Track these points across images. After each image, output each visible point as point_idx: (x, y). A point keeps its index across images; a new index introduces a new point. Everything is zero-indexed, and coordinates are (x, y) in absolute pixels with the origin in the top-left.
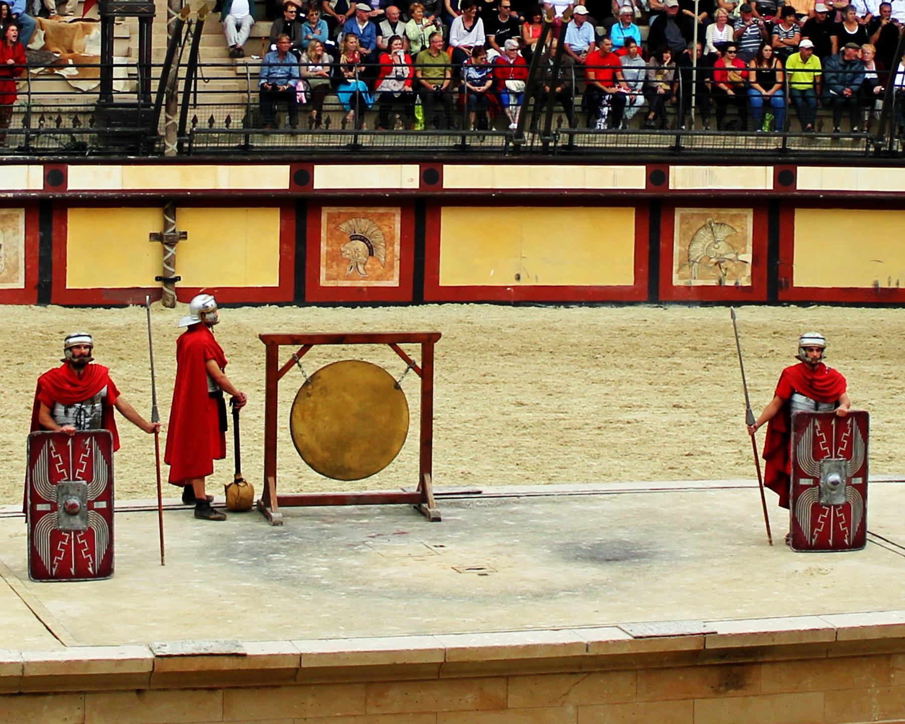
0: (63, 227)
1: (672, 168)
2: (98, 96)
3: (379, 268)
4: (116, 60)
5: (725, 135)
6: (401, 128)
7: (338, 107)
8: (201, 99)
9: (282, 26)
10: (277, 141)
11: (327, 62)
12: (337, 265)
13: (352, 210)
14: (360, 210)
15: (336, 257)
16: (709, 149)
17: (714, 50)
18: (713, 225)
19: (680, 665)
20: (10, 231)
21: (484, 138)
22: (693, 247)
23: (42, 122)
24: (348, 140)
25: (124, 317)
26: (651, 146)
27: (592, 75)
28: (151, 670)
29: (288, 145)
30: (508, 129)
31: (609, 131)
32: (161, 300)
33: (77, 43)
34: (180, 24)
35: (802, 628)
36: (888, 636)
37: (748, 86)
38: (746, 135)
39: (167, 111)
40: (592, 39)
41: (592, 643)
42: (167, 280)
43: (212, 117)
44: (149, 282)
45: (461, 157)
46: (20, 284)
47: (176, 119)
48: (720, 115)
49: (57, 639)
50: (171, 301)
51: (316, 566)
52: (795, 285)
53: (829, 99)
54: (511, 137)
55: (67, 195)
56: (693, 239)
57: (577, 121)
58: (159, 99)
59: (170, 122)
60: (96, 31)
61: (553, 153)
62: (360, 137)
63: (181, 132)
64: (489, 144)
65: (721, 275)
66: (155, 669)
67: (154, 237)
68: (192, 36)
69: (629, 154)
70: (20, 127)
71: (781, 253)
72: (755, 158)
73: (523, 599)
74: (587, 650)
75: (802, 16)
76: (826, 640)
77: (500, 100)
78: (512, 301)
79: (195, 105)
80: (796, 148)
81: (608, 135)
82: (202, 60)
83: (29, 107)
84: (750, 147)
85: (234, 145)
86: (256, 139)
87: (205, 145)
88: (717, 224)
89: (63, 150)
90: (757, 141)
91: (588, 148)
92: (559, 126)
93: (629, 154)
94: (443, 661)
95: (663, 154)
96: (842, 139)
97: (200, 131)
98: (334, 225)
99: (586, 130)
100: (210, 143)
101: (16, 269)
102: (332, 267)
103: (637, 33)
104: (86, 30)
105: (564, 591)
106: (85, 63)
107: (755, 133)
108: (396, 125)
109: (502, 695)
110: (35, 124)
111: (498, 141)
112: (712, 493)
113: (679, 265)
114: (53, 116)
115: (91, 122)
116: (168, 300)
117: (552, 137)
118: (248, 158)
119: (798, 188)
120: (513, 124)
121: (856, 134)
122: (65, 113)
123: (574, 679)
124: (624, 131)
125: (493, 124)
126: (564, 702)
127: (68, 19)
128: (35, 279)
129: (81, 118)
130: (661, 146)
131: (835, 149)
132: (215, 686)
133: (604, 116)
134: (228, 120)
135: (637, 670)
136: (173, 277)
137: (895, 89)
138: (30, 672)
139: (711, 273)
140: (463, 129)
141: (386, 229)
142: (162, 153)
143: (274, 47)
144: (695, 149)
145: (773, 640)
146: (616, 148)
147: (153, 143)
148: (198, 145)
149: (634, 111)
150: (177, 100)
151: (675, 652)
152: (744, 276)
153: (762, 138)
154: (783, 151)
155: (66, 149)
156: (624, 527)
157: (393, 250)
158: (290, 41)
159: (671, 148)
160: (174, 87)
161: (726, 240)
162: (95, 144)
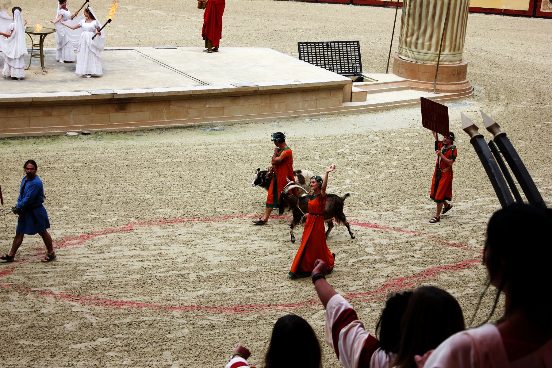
36: (170, 95)
74: (77, 98)
105: (69, 80)
109: (50, 112)
112: (115, 51)
151: (104, 99)
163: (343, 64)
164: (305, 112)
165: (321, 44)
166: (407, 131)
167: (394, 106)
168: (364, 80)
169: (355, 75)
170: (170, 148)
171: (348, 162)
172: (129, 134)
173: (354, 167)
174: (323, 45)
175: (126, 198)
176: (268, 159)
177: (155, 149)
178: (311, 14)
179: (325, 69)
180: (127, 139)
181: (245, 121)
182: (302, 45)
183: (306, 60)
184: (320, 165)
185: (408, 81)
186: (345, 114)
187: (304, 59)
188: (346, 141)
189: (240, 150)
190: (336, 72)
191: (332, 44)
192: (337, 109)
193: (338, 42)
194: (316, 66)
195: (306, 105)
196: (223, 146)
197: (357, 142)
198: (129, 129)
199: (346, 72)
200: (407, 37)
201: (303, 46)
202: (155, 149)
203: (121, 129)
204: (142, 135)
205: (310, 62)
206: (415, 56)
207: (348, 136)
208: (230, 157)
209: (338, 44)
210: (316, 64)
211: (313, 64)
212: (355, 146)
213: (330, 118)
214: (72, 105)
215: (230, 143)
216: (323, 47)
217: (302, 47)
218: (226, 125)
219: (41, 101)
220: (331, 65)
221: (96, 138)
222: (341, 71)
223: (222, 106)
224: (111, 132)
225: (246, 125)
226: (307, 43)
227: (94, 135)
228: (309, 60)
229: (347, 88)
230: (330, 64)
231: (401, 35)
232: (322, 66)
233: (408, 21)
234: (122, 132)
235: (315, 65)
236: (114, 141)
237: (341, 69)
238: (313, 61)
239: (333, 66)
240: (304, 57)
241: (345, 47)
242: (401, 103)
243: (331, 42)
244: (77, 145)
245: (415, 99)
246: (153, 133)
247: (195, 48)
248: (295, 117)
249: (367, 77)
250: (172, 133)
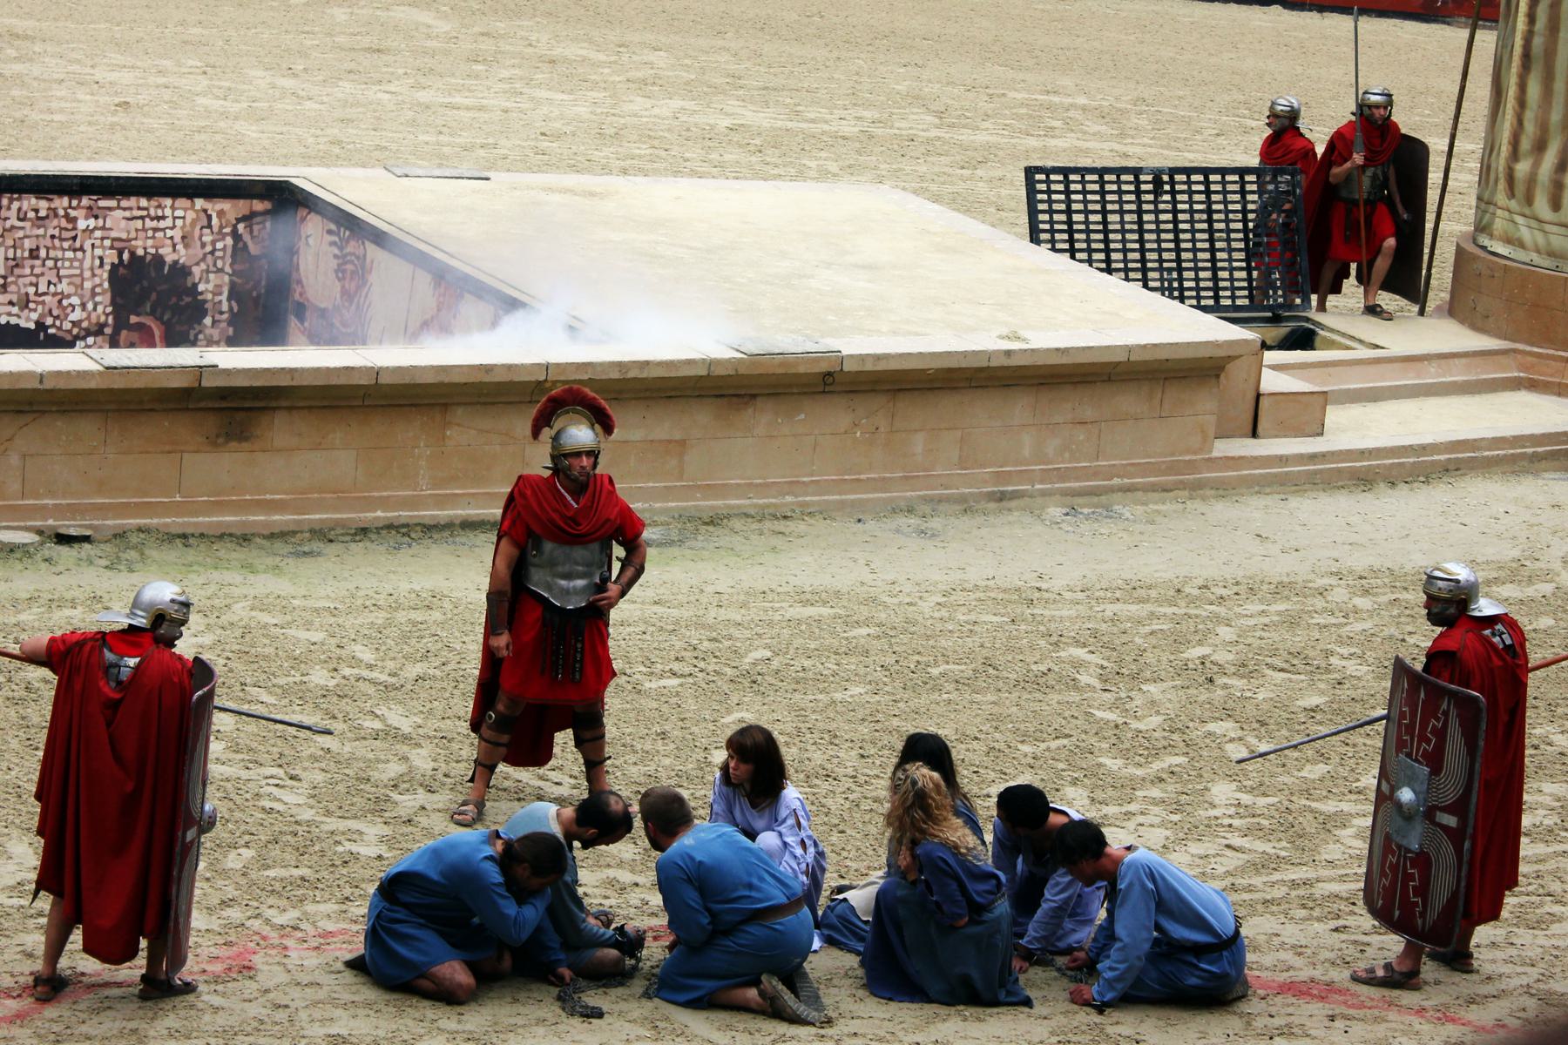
35: (332, 365)
36: (447, 380)
74: (41, 382)
76: (362, 382)
135: (108, 411)
163: (1223, 269)
164: (1046, 476)
165: (1131, 178)
166: (1502, 574)
167: (1449, 459)
168: (1318, 341)
169: (1276, 320)
170: (437, 615)
171: (1230, 704)
172: (261, 548)
173: (1256, 725)
174: (1138, 182)
175: (230, 826)
176: (869, 678)
177: (371, 618)
178: (1096, 44)
179: (1146, 286)
180: (250, 568)
181: (775, 505)
182: (1043, 177)
183: (1059, 246)
184: (1099, 714)
185: (1515, 351)
186: (1224, 489)
187: (1053, 241)
188: (1221, 610)
189: (748, 634)
190: (1194, 302)
191: (1178, 178)
192: (1191, 466)
193: (1206, 172)
194: (1105, 275)
195: (1052, 445)
196: (675, 612)
197: (1276, 618)
198: (266, 524)
199: (1239, 302)
200: (1515, 155)
201: (1048, 182)
202: (371, 618)
203: (229, 524)
204: (319, 554)
205: (1078, 255)
206: (1549, 244)
207: (1236, 589)
208: (702, 665)
209: (1206, 178)
210: (1103, 266)
211: (1090, 262)
212: (1264, 634)
213: (1156, 507)
215: (704, 600)
216: (1138, 192)
217: (1043, 187)
218: (691, 519)
220: (1170, 270)
221: (118, 558)
222: (1217, 298)
223: (677, 436)
224: (184, 536)
225: (783, 522)
226: (1066, 171)
227: (108, 548)
228: (1072, 246)
229: (1236, 374)
230: (1165, 265)
231: (1490, 148)
232: (1132, 275)
233: (1522, 87)
234: (231, 535)
235: (1101, 270)
236: (192, 576)
237: (1216, 289)
238: (1090, 251)
239: (1180, 275)
240: (1052, 231)
241: (1234, 192)
242: (1480, 449)
243: (1173, 171)
244: (32, 588)
245: (1543, 435)
246: (368, 544)
247: (571, 180)
248: (1001, 497)
249: (1332, 330)
250: (452, 547)
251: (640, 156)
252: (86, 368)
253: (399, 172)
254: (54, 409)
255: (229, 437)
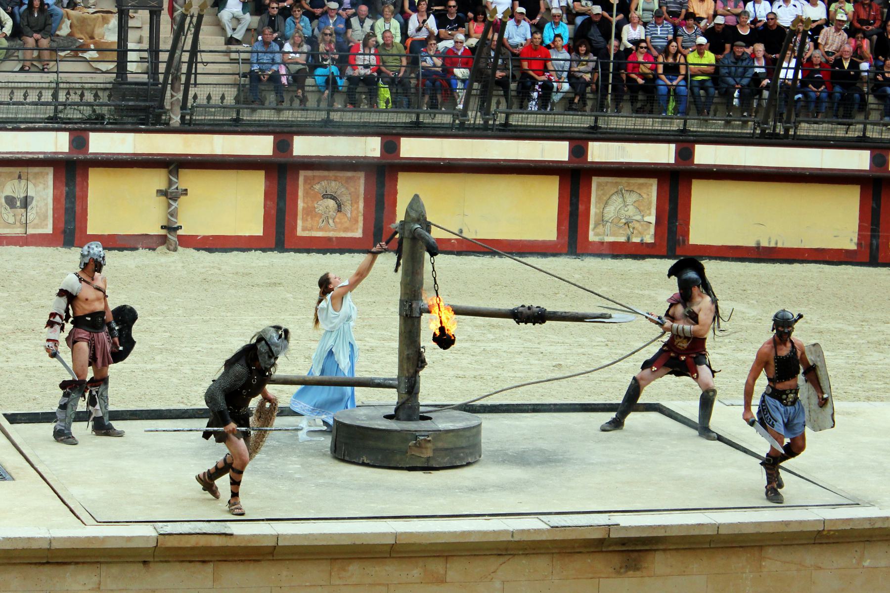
0: (85, 184)
1: (590, 144)
2: (115, 75)
3: (346, 222)
4: (131, 46)
5: (635, 117)
6: (366, 107)
7: (314, 88)
8: (200, 79)
9: (267, 21)
10: (263, 116)
11: (306, 50)
12: (312, 218)
13: (326, 173)
14: (332, 174)
15: (310, 212)
16: (622, 129)
17: (630, 46)
18: (623, 191)
19: (588, 550)
20: (41, 186)
21: (435, 116)
22: (607, 210)
23: (68, 96)
24: (321, 116)
25: (135, 258)
26: (573, 125)
27: (525, 65)
28: (156, 545)
29: (272, 119)
30: (455, 109)
31: (539, 112)
32: (166, 245)
33: (98, 31)
34: (184, 16)
37: (656, 77)
38: (653, 118)
39: (172, 88)
40: (529, 37)
41: (517, 530)
42: (170, 228)
43: (209, 94)
44: (155, 230)
45: (413, 132)
46: (49, 229)
47: (180, 96)
48: (633, 100)
49: (79, 518)
50: (174, 246)
51: (290, 464)
52: (691, 242)
53: (725, 89)
54: (458, 116)
55: (89, 157)
56: (606, 203)
57: (512, 104)
58: (166, 79)
59: (175, 98)
60: (114, 21)
61: (492, 130)
62: (332, 114)
63: (184, 107)
64: (439, 121)
65: (630, 233)
66: (159, 544)
67: (160, 192)
68: (194, 27)
69: (555, 132)
70: (50, 100)
71: (680, 216)
72: (661, 137)
73: (460, 492)
74: (512, 536)
75: (702, 19)
76: (709, 533)
77: (450, 85)
78: (455, 250)
79: (196, 84)
80: (695, 129)
81: (538, 116)
82: (201, 47)
83: (57, 83)
84: (656, 128)
85: (227, 118)
86: (246, 113)
87: (203, 118)
88: (627, 191)
89: (86, 120)
90: (662, 123)
91: (521, 126)
92: (498, 107)
93: (555, 132)
94: (394, 542)
95: (584, 132)
96: (733, 122)
97: (199, 106)
98: (309, 186)
99: (521, 111)
100: (208, 116)
101: (46, 217)
102: (307, 220)
103: (565, 31)
104: (105, 21)
105: (494, 486)
106: (104, 47)
107: (661, 116)
108: (362, 104)
109: (442, 572)
110: (62, 97)
111: (447, 119)
113: (595, 224)
114: (77, 91)
115: (109, 97)
116: (171, 245)
117: (491, 117)
118: (239, 129)
119: (696, 162)
120: (459, 106)
121: (745, 119)
122: (87, 89)
123: (501, 560)
124: (552, 112)
125: (442, 105)
126: (492, 579)
127: (91, 10)
128: (62, 225)
129: (100, 93)
130: (582, 125)
131: (727, 131)
132: (207, 559)
133: (534, 100)
134: (223, 98)
135: (553, 553)
136: (175, 226)
137: (779, 81)
138: (55, 545)
139: (621, 231)
140: (418, 108)
141: (353, 190)
142: (168, 124)
143: (260, 38)
144: (611, 129)
145: (666, 532)
146: (544, 127)
147: (160, 115)
148: (197, 118)
149: (560, 95)
150: (180, 80)
151: (584, 540)
152: (649, 234)
153: (666, 120)
154: (684, 131)
155: (88, 119)
156: (543, 438)
157: (358, 207)
158: (274, 31)
159: (591, 127)
160: (178, 69)
161: (636, 204)
162: (112, 115)
214: (499, 555)
219: (418, 541)
251: (878, 389)
252: (539, 528)
253: (727, 402)
254: (521, 553)
255: (628, 568)
